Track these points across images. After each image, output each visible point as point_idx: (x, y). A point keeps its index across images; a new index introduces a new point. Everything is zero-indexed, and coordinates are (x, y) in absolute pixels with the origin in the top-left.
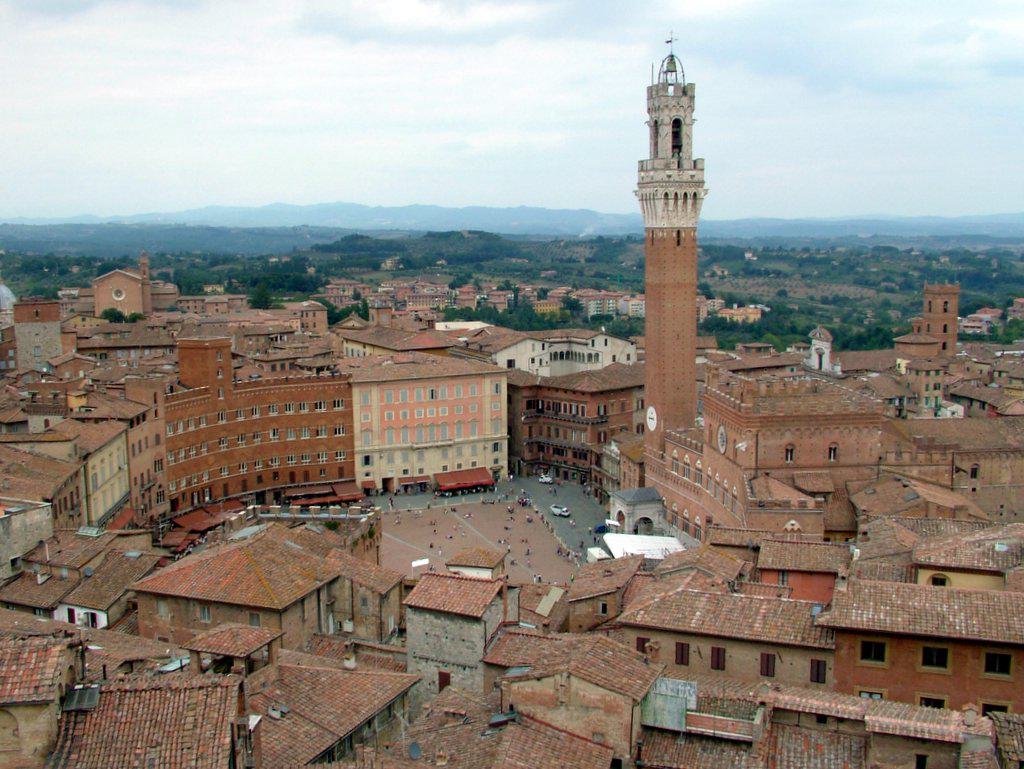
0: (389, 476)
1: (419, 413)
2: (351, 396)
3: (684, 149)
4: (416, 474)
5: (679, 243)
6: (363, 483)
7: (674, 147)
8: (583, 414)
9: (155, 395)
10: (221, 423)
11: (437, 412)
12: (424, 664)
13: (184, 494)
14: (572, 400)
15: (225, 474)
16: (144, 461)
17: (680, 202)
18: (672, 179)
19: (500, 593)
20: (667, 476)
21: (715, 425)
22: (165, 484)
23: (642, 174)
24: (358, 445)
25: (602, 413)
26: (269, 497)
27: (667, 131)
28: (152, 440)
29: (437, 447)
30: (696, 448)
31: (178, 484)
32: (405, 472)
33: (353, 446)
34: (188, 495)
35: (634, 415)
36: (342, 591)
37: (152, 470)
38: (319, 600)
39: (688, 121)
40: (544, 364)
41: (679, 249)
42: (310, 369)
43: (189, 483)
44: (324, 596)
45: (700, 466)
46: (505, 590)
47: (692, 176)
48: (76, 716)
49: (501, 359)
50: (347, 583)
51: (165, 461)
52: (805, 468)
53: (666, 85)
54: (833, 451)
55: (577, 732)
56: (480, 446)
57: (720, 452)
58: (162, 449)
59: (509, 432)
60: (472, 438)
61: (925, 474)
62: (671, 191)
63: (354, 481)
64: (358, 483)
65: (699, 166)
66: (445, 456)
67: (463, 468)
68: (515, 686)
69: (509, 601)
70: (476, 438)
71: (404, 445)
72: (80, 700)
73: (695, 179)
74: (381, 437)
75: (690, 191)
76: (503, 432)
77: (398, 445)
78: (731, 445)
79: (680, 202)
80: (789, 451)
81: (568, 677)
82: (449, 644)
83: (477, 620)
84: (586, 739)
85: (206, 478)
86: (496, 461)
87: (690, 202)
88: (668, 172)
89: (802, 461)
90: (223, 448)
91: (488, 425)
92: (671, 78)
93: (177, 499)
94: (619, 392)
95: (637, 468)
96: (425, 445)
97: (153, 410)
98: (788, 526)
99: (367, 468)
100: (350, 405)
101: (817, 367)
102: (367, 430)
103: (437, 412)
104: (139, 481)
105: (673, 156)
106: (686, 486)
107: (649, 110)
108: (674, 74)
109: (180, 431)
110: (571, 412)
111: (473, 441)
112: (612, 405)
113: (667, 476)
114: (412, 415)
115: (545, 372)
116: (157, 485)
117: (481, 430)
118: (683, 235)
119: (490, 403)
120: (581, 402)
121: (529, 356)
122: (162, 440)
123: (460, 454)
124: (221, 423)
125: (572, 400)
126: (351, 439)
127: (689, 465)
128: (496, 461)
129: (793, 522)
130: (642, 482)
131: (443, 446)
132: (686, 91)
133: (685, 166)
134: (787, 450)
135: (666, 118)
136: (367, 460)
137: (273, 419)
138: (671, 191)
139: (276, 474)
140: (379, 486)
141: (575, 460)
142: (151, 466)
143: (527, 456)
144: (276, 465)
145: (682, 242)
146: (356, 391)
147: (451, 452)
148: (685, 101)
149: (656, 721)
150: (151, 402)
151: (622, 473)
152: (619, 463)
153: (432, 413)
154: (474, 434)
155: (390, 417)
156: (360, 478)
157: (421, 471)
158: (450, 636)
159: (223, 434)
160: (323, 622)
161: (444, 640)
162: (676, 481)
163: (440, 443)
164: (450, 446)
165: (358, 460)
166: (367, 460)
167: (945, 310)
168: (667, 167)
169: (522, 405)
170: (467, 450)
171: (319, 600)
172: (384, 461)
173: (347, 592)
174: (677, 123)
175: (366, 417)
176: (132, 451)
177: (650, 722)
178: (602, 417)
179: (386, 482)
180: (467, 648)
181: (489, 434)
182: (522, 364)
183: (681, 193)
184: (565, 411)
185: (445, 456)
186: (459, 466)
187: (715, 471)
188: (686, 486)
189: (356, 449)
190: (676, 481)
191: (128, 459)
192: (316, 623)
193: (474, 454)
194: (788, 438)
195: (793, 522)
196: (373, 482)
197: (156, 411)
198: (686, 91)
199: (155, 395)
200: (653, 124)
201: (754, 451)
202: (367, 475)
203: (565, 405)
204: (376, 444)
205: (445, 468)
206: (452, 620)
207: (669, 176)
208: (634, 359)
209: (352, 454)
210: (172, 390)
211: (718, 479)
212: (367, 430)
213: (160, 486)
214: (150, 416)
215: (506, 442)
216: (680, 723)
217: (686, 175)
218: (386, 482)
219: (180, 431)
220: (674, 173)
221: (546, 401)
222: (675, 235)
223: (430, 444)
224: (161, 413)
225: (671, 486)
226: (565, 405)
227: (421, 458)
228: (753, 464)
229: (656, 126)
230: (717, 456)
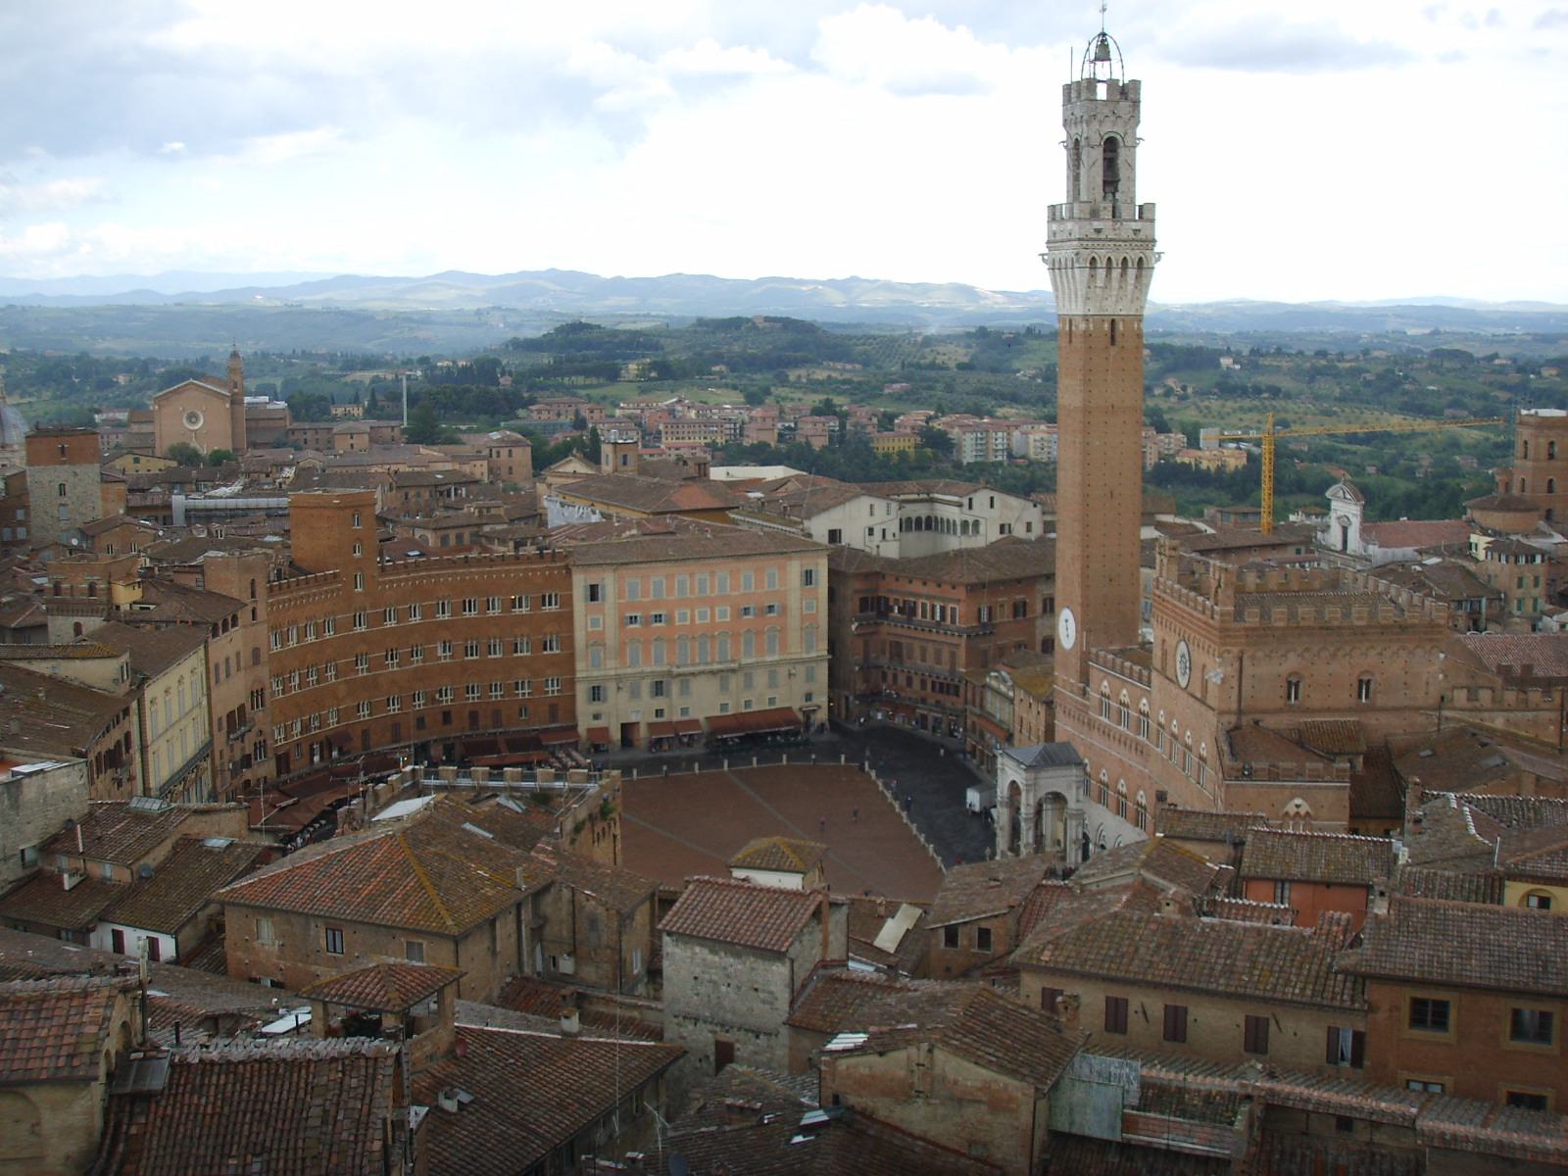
0: (633, 719)
1: (683, 617)
2: (570, 587)
3: (1121, 186)
4: (677, 717)
5: (1113, 338)
6: (589, 730)
7: (1105, 183)
8: (953, 621)
9: (253, 582)
10: (358, 630)
11: (713, 615)
12: (691, 1027)
13: (298, 744)
14: (934, 598)
15: (364, 714)
16: (233, 693)
17: (1116, 273)
18: (1102, 236)
19: (817, 915)
20: (1091, 725)
21: (1172, 639)
22: (267, 729)
23: (1054, 227)
24: (581, 666)
25: (985, 618)
26: (436, 751)
27: (1094, 156)
28: (246, 657)
29: (712, 673)
30: (1140, 680)
31: (288, 730)
32: (659, 713)
33: (573, 671)
34: (305, 748)
35: (1038, 622)
36: (555, 908)
37: (248, 706)
38: (519, 921)
39: (1129, 141)
40: (889, 536)
41: (1113, 350)
42: (503, 542)
43: (306, 728)
44: (526, 914)
45: (1146, 709)
46: (825, 908)
47: (1136, 231)
48: (132, 1104)
49: (819, 527)
50: (566, 894)
51: (267, 693)
52: (1320, 711)
53: (1092, 83)
54: (1364, 685)
55: (943, 1141)
56: (783, 671)
57: (1177, 683)
58: (263, 672)
59: (832, 649)
60: (768, 659)
61: (1516, 725)
62: (1102, 254)
63: (574, 727)
64: (582, 729)
65: (1146, 215)
66: (724, 687)
67: (755, 708)
68: (843, 1064)
69: (831, 926)
70: (776, 658)
71: (659, 669)
72: (140, 1076)
73: (1141, 236)
74: (620, 653)
75: (1133, 256)
76: (822, 649)
78: (1197, 674)
79: (1116, 273)
80: (1292, 685)
81: (930, 1051)
82: (732, 995)
83: (779, 956)
84: (957, 1152)
85: (333, 722)
86: (809, 697)
87: (1132, 273)
88: (1097, 224)
89: (1380, 701)
90: (362, 671)
91: (794, 636)
92: (1102, 71)
93: (287, 755)
94: (1017, 583)
95: (1042, 709)
96: (691, 669)
97: (249, 608)
98: (1291, 808)
99: (597, 707)
100: (568, 602)
101: (1339, 547)
102: (595, 644)
103: (713, 615)
104: (224, 720)
105: (1104, 198)
106: (1122, 740)
107: (1066, 123)
108: (1107, 63)
109: (293, 644)
110: (933, 617)
111: (772, 664)
112: (1002, 606)
113: (1091, 725)
115: (891, 550)
116: (255, 730)
117: (784, 647)
118: (1120, 327)
119: (799, 593)
120: (952, 600)
121: (864, 521)
122: (264, 658)
123: (749, 684)
124: (358, 630)
125: (934, 598)
126: (570, 658)
127: (1127, 706)
128: (809, 697)
129: (1298, 801)
130: (1050, 731)
131: (722, 671)
132: (1127, 94)
133: (1125, 215)
134: (1290, 683)
135: (1096, 133)
136: (596, 694)
137: (443, 624)
138: (1102, 254)
139: (447, 717)
140: (616, 735)
141: (940, 697)
142: (243, 698)
143: (861, 687)
144: (447, 700)
145: (1118, 338)
146: (580, 582)
147: (735, 682)
148: (1124, 106)
149: (1072, 1124)
150: (246, 598)
151: (1017, 720)
152: (1011, 701)
153: (703, 616)
154: (772, 651)
156: (584, 724)
157: (684, 711)
158: (734, 983)
159: (364, 648)
160: (525, 958)
161: (724, 989)
162: (1106, 732)
163: (716, 667)
164: (733, 671)
165: (582, 692)
166: (596, 694)
167: (1551, 456)
168: (1094, 214)
169: (851, 606)
170: (761, 679)
171: (519, 921)
172: (624, 695)
173: (565, 910)
174: (1111, 146)
175: (595, 623)
176: (212, 675)
177: (1062, 1125)
178: (984, 626)
179: (627, 728)
180: (764, 1002)
181: (796, 650)
182: (854, 537)
183: (1117, 258)
184: (924, 615)
185: (724, 687)
186: (748, 704)
187: (1170, 716)
188: (1122, 740)
189: (578, 675)
190: (1106, 732)
191: (209, 688)
192: (515, 960)
193: (773, 683)
194: (1292, 663)
195: (1298, 801)
196: (605, 730)
197: (254, 611)
198: (1127, 94)
199: (253, 582)
200: (1071, 146)
201: (1235, 683)
202: (596, 717)
203: (924, 605)
204: (611, 667)
205: (724, 707)
206: (738, 955)
207: (1098, 231)
208: (1037, 530)
210: (279, 577)
211: (1175, 730)
212: (596, 641)
214: (244, 616)
215: (825, 665)
216: (1113, 1128)
217: (1126, 230)
218: (627, 728)
219: (293, 644)
220: (1105, 224)
221: (892, 597)
222: (1107, 326)
223: (702, 668)
224: (262, 614)
225: (1097, 741)
226: (924, 605)
227: (685, 690)
228: (1234, 706)
229: (1075, 149)
230: (1175, 691)
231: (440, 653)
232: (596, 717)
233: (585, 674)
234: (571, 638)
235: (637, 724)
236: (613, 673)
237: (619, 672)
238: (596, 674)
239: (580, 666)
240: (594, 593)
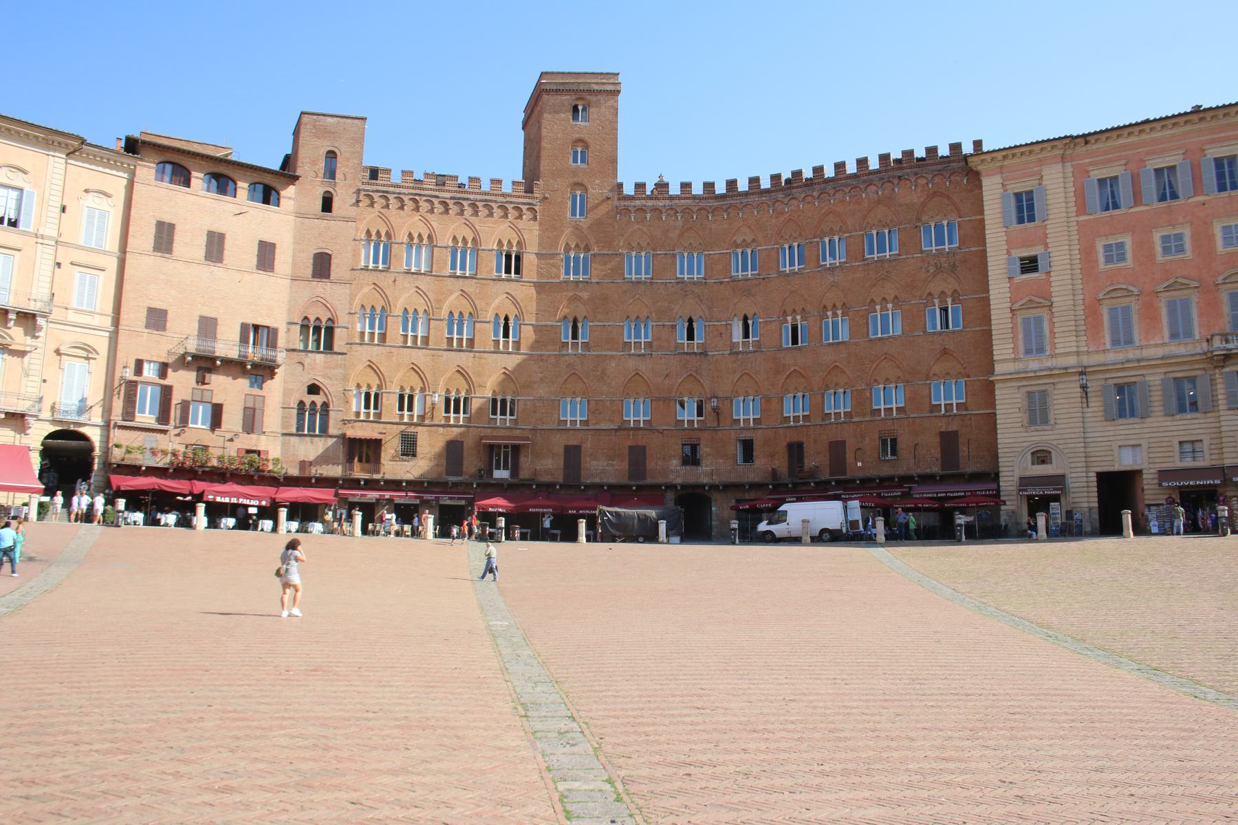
0: (1125, 462)
6: (1025, 482)
32: (1189, 446)
64: (1008, 483)
77: (1160, 352)
114: (1203, 240)
136: (1038, 411)
137: (744, 288)
140: (1084, 497)
146: (992, 188)
155: (1115, 253)
156: (1014, 468)
165: (1009, 406)
166: (1038, 411)
189: (998, 368)
196: (1059, 480)
209: (990, 388)
213: (313, 389)
231: (737, 335)
232: (1042, 457)
233: (1011, 367)
234: (985, 303)
235: (1139, 472)
236: (1071, 361)
237: (1086, 360)
238: (1034, 365)
239: (1002, 349)
240: (1026, 207)
